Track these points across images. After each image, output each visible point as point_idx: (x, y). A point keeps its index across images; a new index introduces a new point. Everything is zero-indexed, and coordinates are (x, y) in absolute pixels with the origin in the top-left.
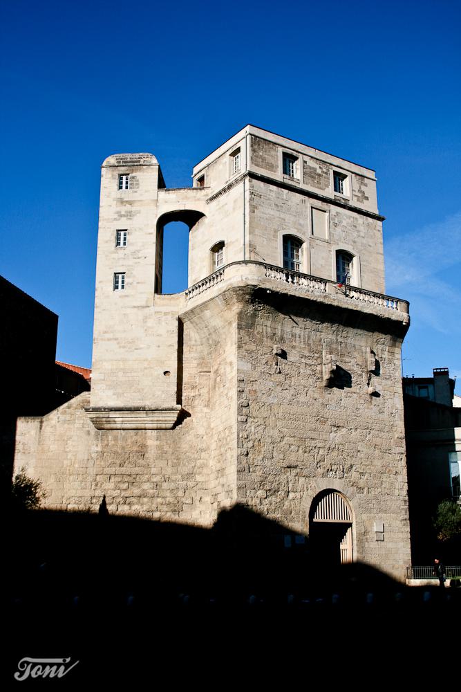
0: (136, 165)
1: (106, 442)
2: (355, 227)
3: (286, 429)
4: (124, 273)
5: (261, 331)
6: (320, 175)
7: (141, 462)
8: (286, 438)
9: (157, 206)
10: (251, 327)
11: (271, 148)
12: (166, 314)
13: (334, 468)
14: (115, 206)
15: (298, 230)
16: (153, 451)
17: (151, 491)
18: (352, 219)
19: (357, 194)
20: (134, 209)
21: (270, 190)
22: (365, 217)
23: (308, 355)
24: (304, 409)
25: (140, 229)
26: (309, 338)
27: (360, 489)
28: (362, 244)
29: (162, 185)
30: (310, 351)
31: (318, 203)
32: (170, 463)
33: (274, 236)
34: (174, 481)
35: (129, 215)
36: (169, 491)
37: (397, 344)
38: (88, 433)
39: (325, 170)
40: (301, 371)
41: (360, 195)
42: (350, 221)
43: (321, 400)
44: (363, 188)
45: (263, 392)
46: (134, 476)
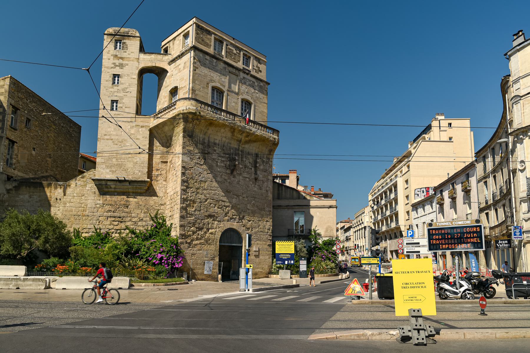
0: (127, 36)
1: (105, 199)
3: (208, 195)
4: (118, 101)
7: (126, 210)
8: (208, 200)
9: (138, 62)
12: (142, 127)
14: (112, 59)
16: (133, 205)
17: (132, 226)
20: (124, 62)
23: (222, 155)
25: (128, 75)
29: (142, 50)
32: (143, 211)
34: (146, 221)
35: (121, 66)
36: (142, 227)
38: (95, 193)
40: (219, 164)
46: (122, 218)
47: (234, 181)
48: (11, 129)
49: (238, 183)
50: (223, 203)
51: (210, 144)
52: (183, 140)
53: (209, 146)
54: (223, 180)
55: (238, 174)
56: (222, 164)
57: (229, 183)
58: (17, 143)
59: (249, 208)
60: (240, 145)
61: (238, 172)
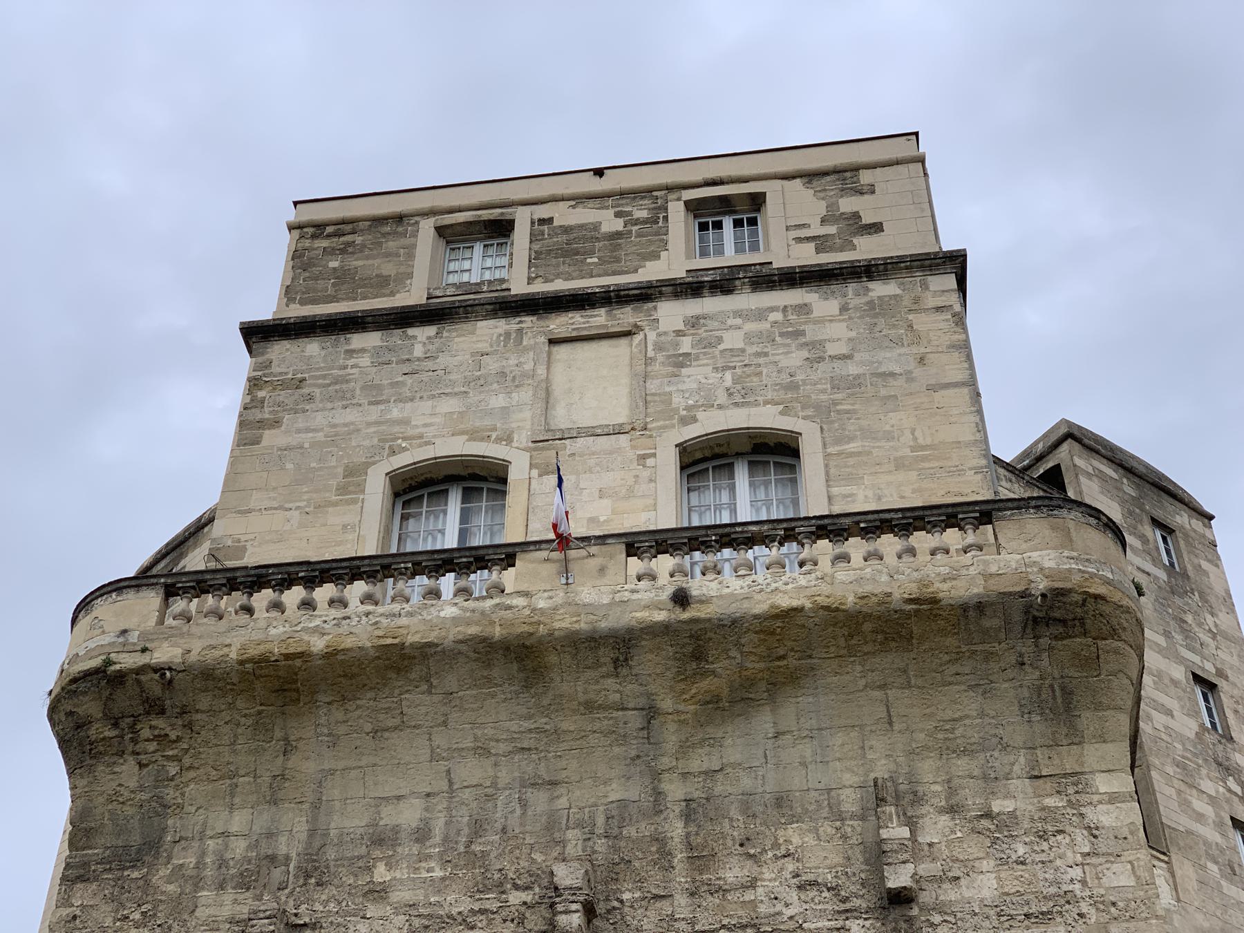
2: (798, 334)
5: (191, 860)
6: (617, 235)
10: (136, 863)
11: (384, 235)
15: (475, 435)
19: (817, 230)
22: (852, 287)
23: (465, 905)
26: (478, 828)
31: (599, 318)
33: (342, 490)
37: (1087, 720)
41: (831, 230)
42: (765, 326)
44: (847, 204)
51: (331, 854)
52: (64, 900)
60: (666, 762)
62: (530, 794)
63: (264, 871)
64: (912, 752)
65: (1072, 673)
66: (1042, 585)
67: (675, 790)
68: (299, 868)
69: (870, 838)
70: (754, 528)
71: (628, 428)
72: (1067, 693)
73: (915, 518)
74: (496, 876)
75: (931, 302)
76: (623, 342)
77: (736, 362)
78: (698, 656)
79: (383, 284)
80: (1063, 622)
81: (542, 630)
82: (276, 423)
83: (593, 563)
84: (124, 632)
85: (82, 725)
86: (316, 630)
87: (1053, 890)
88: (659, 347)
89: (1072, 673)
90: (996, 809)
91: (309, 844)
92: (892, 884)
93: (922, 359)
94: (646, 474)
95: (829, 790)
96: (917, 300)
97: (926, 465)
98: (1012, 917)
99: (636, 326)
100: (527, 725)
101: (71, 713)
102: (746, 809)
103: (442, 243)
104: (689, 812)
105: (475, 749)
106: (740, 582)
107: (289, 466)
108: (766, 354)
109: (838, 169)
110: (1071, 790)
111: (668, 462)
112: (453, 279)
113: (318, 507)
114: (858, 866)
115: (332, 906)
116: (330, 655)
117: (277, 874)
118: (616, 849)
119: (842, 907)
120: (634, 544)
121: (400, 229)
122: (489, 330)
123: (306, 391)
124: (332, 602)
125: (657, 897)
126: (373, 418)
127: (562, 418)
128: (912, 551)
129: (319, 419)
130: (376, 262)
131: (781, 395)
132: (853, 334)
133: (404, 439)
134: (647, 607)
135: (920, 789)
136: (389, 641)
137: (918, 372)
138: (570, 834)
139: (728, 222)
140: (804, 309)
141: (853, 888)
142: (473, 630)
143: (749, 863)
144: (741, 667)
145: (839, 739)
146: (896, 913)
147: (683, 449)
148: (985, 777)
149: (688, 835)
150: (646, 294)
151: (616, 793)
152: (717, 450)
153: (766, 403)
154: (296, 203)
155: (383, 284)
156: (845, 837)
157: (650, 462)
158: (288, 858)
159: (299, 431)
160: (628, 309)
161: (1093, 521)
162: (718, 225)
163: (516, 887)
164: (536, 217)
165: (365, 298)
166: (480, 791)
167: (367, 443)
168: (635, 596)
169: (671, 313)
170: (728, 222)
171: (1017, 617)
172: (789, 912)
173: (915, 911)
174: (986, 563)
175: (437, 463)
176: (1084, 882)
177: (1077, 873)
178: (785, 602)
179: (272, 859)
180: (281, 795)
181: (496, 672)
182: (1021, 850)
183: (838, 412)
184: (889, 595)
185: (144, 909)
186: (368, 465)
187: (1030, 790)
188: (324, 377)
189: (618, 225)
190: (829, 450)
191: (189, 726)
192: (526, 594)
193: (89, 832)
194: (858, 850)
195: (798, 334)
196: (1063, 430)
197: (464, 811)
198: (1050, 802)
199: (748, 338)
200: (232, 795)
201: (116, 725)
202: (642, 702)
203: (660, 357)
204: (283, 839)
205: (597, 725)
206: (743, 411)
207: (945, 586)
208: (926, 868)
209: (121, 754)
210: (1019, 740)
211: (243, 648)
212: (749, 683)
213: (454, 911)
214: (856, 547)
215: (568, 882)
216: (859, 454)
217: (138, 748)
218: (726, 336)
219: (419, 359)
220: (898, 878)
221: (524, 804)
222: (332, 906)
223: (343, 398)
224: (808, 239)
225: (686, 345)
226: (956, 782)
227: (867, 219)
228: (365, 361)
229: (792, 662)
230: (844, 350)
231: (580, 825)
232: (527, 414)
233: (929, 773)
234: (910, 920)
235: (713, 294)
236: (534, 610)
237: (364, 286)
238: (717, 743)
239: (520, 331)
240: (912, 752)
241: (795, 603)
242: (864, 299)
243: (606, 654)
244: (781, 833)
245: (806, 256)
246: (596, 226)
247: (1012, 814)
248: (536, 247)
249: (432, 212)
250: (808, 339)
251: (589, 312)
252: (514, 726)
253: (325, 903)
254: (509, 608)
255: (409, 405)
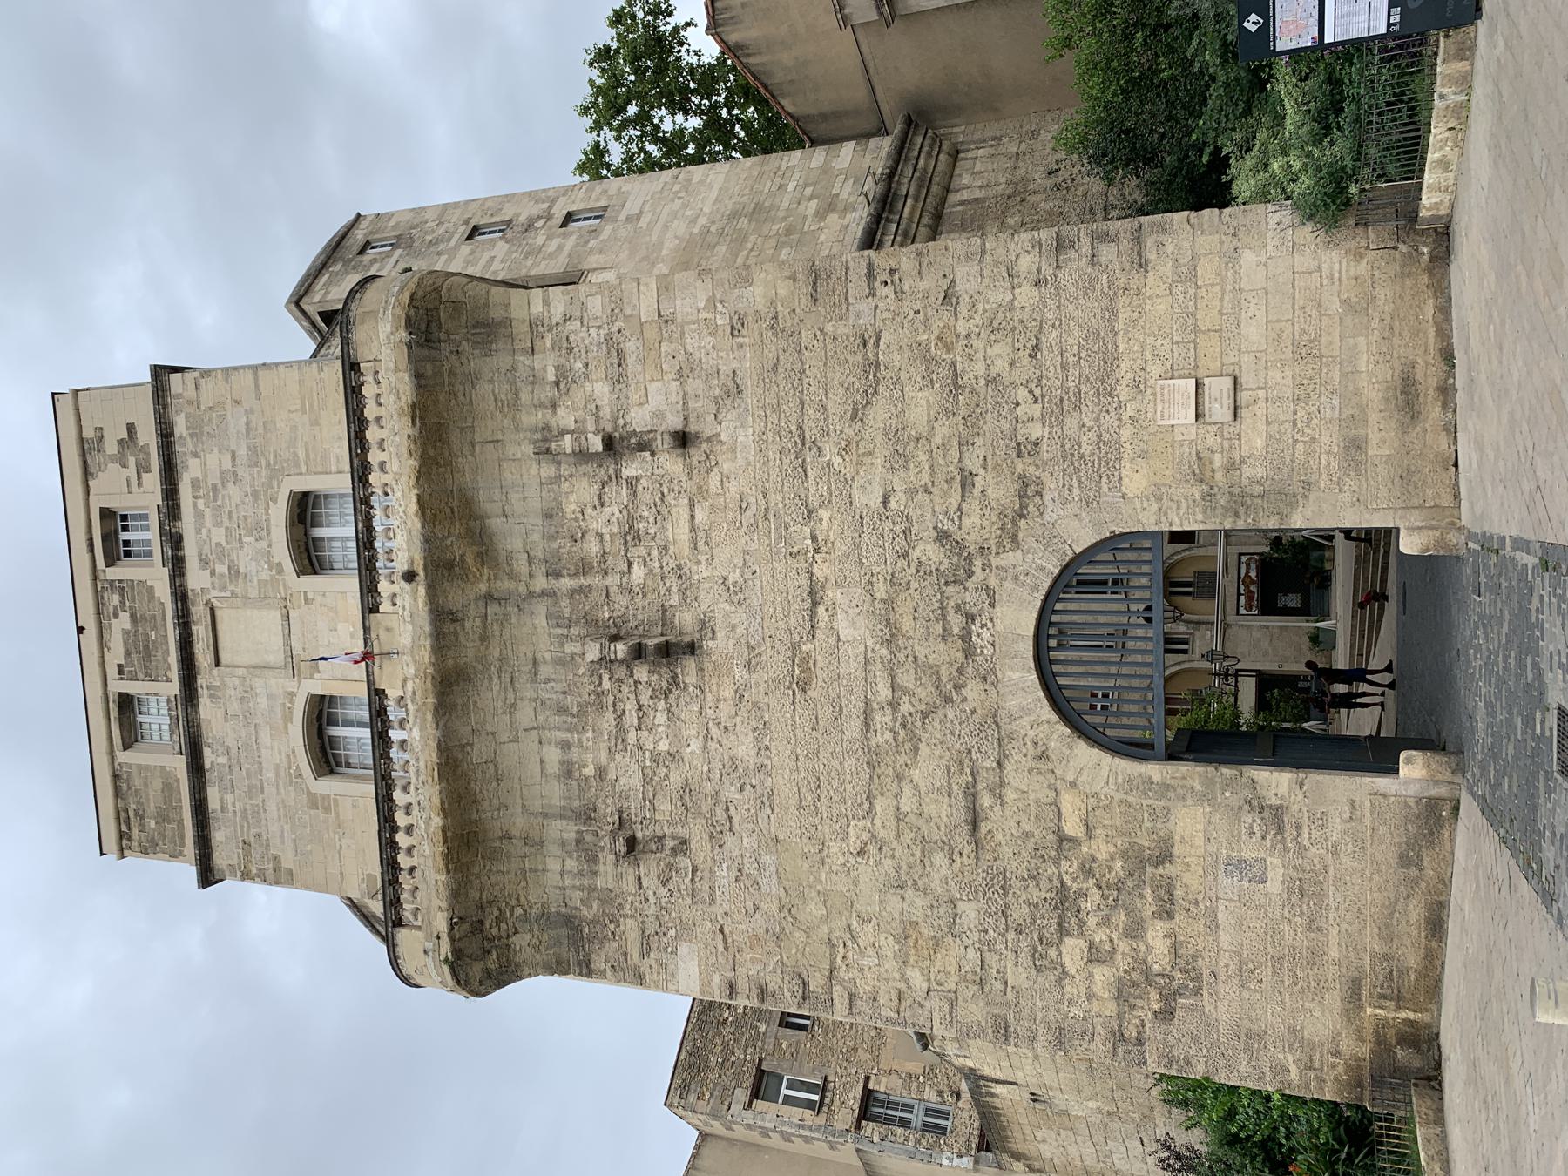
2: (215, 489)
5: (578, 894)
6: (133, 617)
8: (882, 833)
10: (579, 930)
11: (129, 788)
13: (956, 622)
15: (288, 718)
18: (200, 503)
19: (132, 471)
21: (223, 809)
22: (178, 448)
23: (610, 716)
24: (781, 753)
26: (562, 710)
27: (1027, 490)
28: (255, 452)
30: (600, 707)
31: (200, 631)
33: (327, 810)
37: (496, 314)
39: (116, 598)
40: (663, 746)
41: (132, 461)
42: (208, 512)
43: (740, 674)
44: (111, 447)
45: (749, 904)
47: (733, 628)
48: (825, 1109)
49: (736, 594)
50: (881, 718)
51: (576, 804)
52: (602, 975)
53: (587, 815)
54: (743, 712)
55: (684, 601)
56: (661, 718)
57: (749, 666)
58: (867, 1079)
59: (875, 500)
60: (522, 589)
61: (674, 600)
62: (542, 676)
63: (586, 846)
64: (517, 428)
65: (463, 321)
66: (403, 334)
67: (540, 583)
68: (584, 824)
69: (572, 460)
70: (360, 526)
71: (284, 611)
72: (477, 325)
73: (355, 415)
74: (593, 697)
75: (191, 392)
76: (218, 613)
77: (235, 534)
78: (450, 565)
79: (169, 788)
80: (429, 322)
81: (431, 670)
82: (276, 858)
83: (383, 635)
84: (425, 952)
85: (488, 974)
86: (427, 824)
87: (604, 347)
88: (223, 588)
89: (463, 321)
90: (554, 379)
91: (569, 818)
92: (600, 448)
93: (237, 402)
94: (319, 599)
95: (541, 483)
96: (190, 403)
97: (316, 408)
98: (620, 375)
99: (206, 604)
100: (495, 680)
101: (481, 982)
102: (553, 538)
103: (136, 745)
104: (555, 574)
105: (511, 713)
106: (399, 537)
107: (309, 848)
108: (230, 512)
109: (81, 452)
110: (541, 329)
111: (311, 583)
112: (166, 736)
113: (339, 827)
114: (589, 468)
115: (609, 801)
116: (444, 812)
117: (588, 838)
118: (578, 621)
119: (614, 479)
120: (370, 606)
121: (125, 776)
122: (207, 708)
123: (252, 839)
124: (408, 814)
125: (608, 596)
126: (274, 790)
127: (276, 657)
128: (378, 419)
129: (274, 828)
130: (151, 793)
131: (262, 504)
132: (216, 450)
133: (290, 768)
134: (415, 600)
135: (541, 425)
136: (436, 773)
137: (246, 405)
138: (568, 650)
139: (124, 536)
140: (195, 484)
141: (603, 472)
142: (429, 717)
143: (587, 537)
144: (459, 537)
145: (507, 475)
146: (617, 447)
147: (301, 572)
148: (533, 383)
149: (569, 575)
150: (181, 597)
151: (541, 621)
152: (302, 549)
153: (267, 513)
154: (102, 854)
155: (169, 788)
156: (571, 476)
157: (310, 596)
158: (578, 832)
159: (283, 843)
160: (193, 610)
161: (358, 295)
162: (126, 543)
163: (600, 684)
164: (117, 677)
165: (180, 801)
166: (539, 709)
167: (293, 794)
168: (407, 608)
169: (196, 579)
170: (124, 536)
171: (425, 352)
172: (617, 513)
173: (617, 435)
174: (387, 370)
175: (309, 744)
176: (599, 327)
177: (593, 331)
178: (413, 507)
179: (578, 842)
180: (537, 839)
181: (459, 701)
182: (579, 365)
183: (275, 463)
184: (409, 436)
185: (607, 922)
186: (309, 793)
187: (541, 356)
188: (242, 827)
189: (125, 617)
190: (304, 470)
191: (490, 903)
192: (405, 681)
193: (559, 963)
194: (579, 468)
195: (215, 489)
196: (293, 307)
197: (551, 719)
198: (549, 344)
199: (217, 524)
200: (536, 871)
201: (489, 952)
202: (481, 603)
203: (231, 587)
204: (566, 836)
205: (497, 633)
206: (273, 529)
207: (403, 399)
208: (591, 426)
209: (508, 946)
210: (509, 360)
211: (438, 871)
212: (469, 532)
213: (614, 723)
214: (374, 457)
215: (597, 652)
216: (307, 450)
217: (503, 934)
218: (215, 540)
219: (230, 759)
220: (596, 444)
221: (548, 680)
222: (609, 801)
223: (258, 813)
224: (139, 478)
225: (222, 569)
226: (536, 402)
227: (125, 435)
228: (230, 798)
229: (455, 503)
230: (229, 456)
231: (562, 644)
232: (273, 681)
233: (530, 419)
234: (622, 438)
235: (182, 549)
236: (416, 676)
237: (171, 801)
238: (510, 556)
239: (208, 687)
240: (517, 428)
241: (414, 499)
242: (188, 439)
243: (449, 627)
244: (568, 516)
245: (153, 480)
246: (125, 632)
247: (557, 368)
248: (141, 676)
249: (111, 753)
250: (218, 482)
251: (195, 638)
252: (496, 688)
253: (607, 806)
254: (414, 693)
255: (264, 765)
